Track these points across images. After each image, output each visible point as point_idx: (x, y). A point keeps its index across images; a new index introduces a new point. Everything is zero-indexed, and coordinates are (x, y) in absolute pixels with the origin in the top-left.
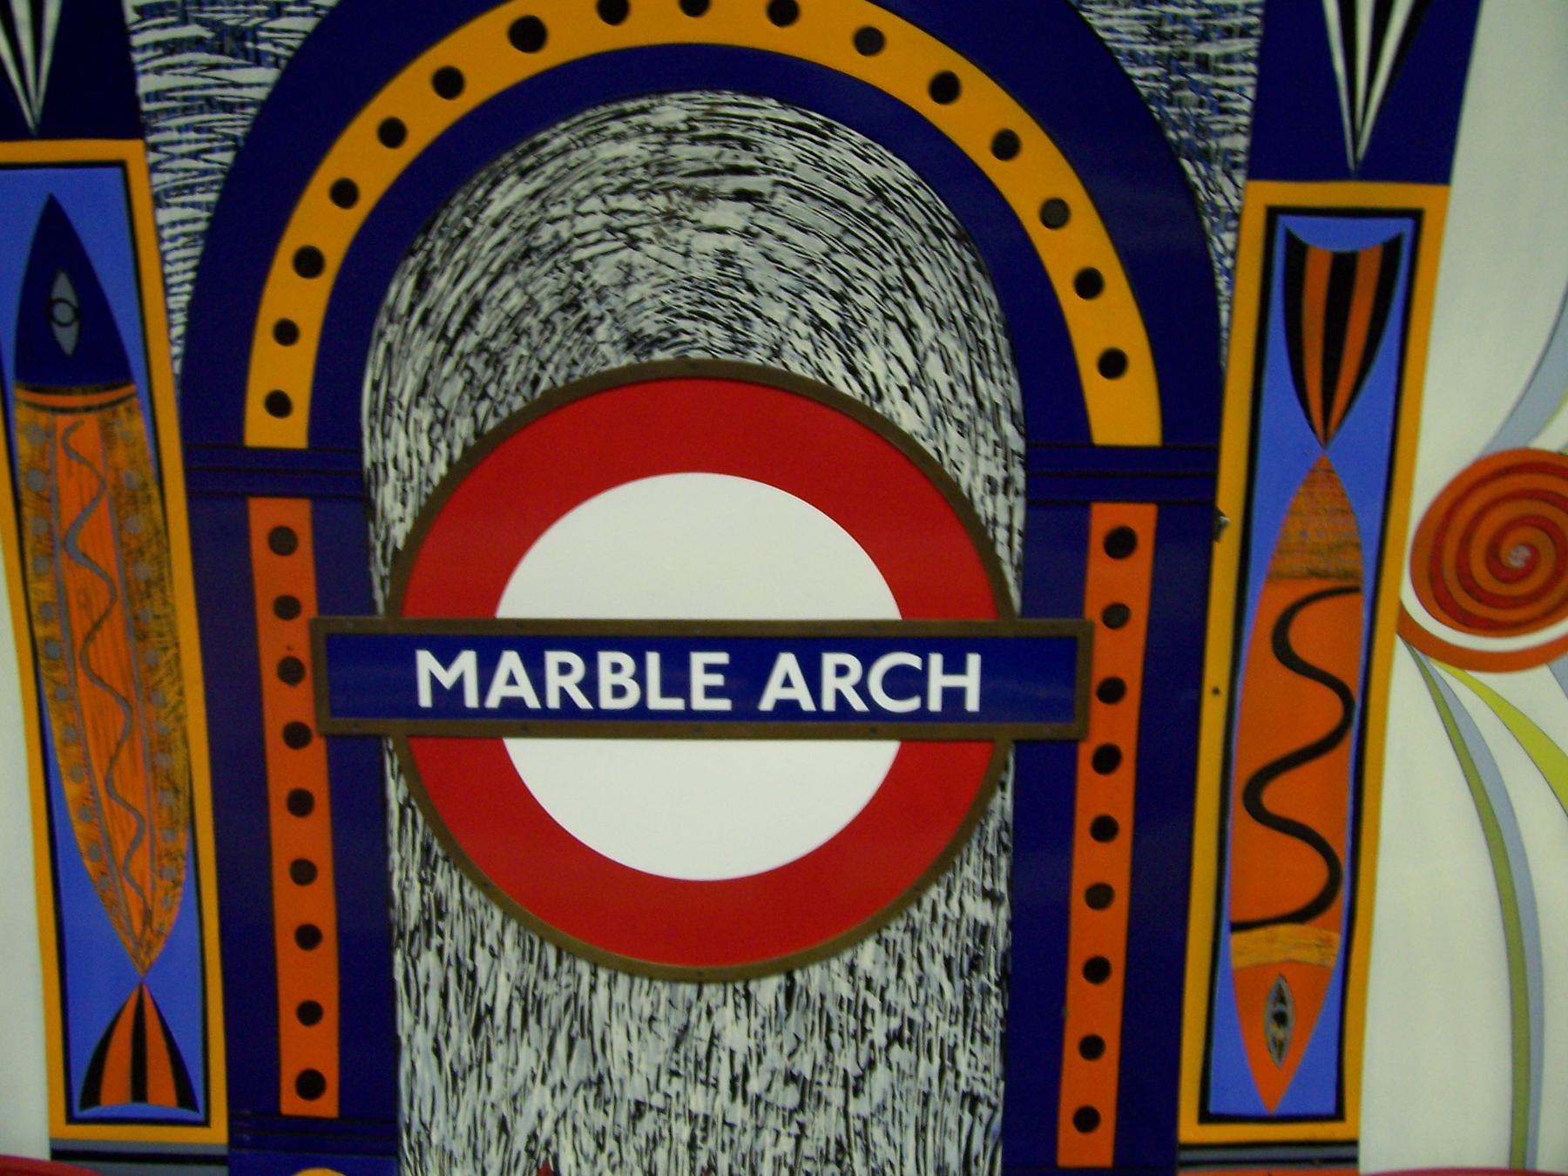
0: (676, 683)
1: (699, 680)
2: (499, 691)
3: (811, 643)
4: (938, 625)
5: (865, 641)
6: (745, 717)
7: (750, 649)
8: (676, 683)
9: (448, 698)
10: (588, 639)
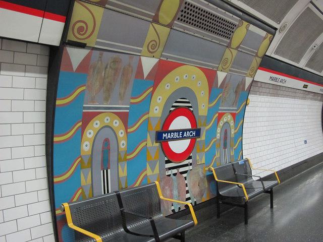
0: (179, 136)
1: (181, 135)
2: (168, 137)
3: (186, 130)
4: (194, 128)
5: (189, 130)
6: (183, 138)
7: (184, 131)
8: (179, 136)
9: (165, 138)
10: (174, 131)
